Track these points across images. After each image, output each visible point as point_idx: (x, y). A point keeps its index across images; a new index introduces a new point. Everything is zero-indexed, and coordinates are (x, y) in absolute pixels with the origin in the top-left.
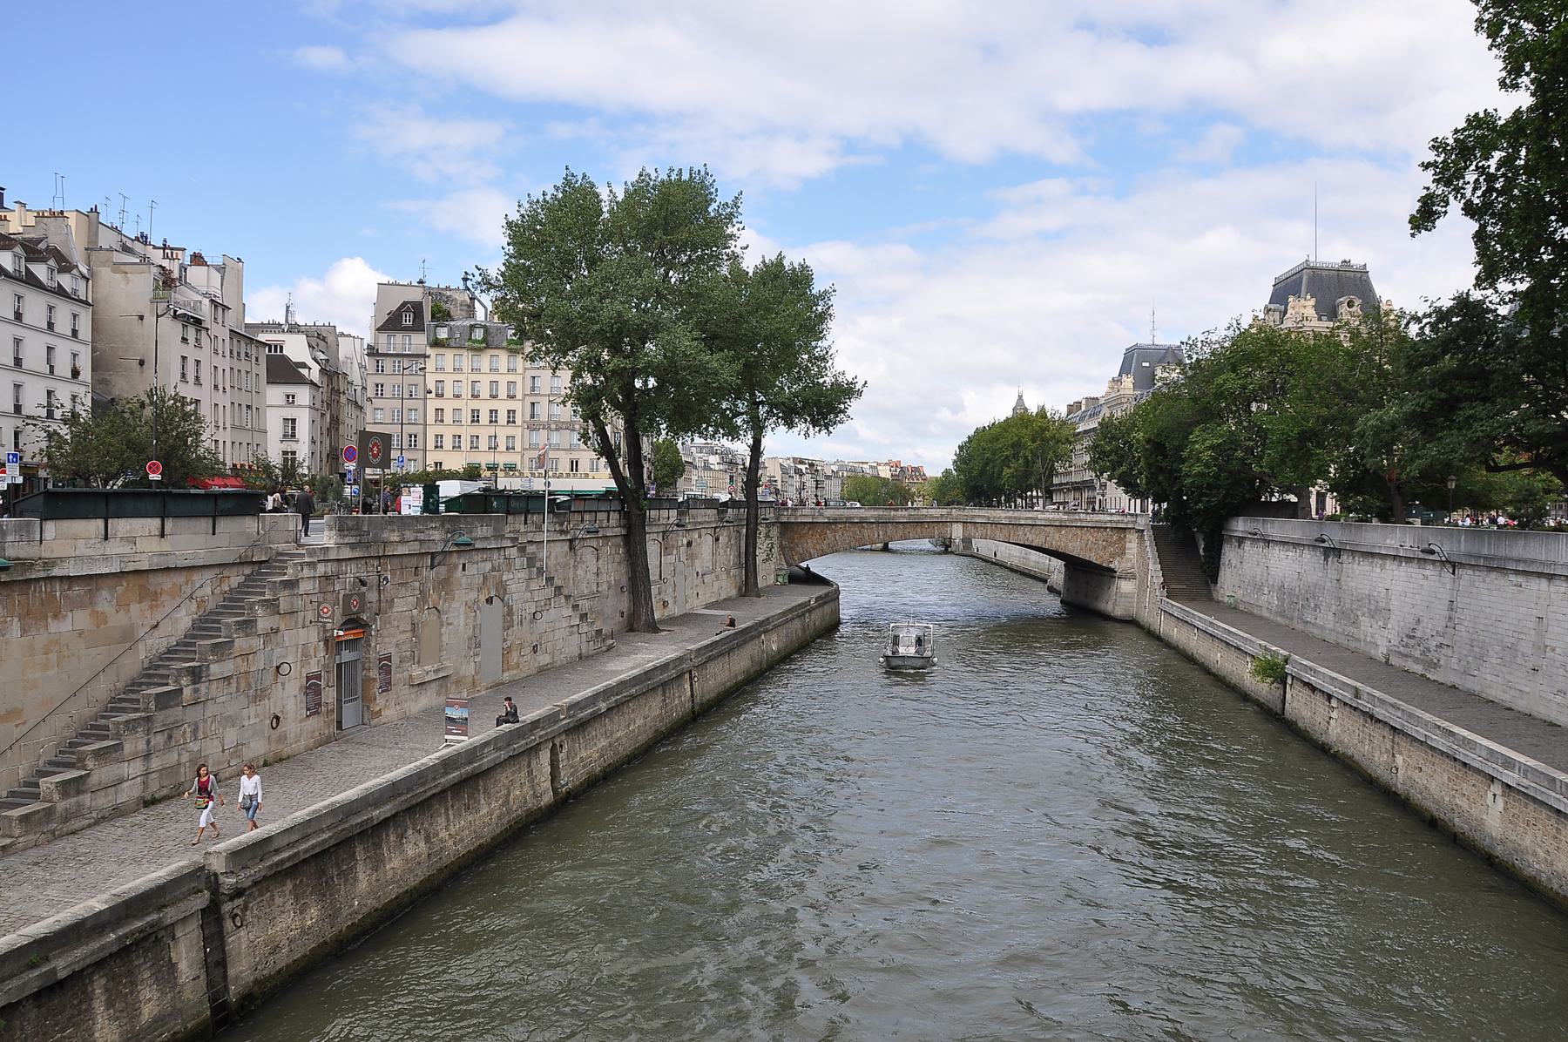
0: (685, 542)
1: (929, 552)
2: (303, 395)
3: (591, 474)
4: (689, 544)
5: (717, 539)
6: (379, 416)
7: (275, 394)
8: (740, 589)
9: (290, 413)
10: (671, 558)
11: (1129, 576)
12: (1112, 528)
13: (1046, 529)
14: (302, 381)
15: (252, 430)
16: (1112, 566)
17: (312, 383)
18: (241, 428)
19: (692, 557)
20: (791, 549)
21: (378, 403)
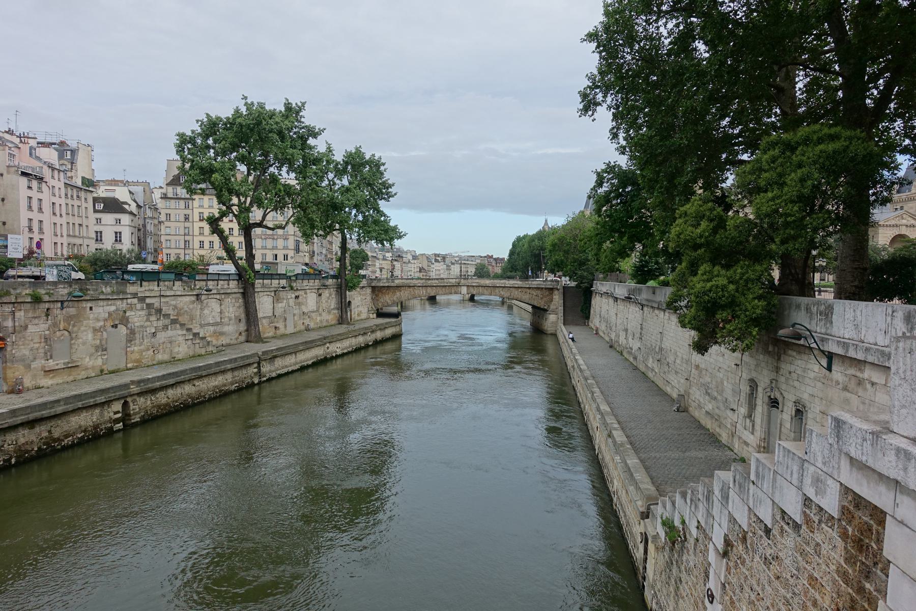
0: (293, 296)
2: (125, 219)
4: (297, 297)
5: (320, 295)
6: (168, 231)
7: (109, 218)
9: (118, 229)
10: (280, 305)
12: (546, 289)
14: (124, 211)
15: (83, 237)
17: (131, 213)
18: (75, 236)
19: (299, 304)
20: (378, 300)
21: (167, 224)
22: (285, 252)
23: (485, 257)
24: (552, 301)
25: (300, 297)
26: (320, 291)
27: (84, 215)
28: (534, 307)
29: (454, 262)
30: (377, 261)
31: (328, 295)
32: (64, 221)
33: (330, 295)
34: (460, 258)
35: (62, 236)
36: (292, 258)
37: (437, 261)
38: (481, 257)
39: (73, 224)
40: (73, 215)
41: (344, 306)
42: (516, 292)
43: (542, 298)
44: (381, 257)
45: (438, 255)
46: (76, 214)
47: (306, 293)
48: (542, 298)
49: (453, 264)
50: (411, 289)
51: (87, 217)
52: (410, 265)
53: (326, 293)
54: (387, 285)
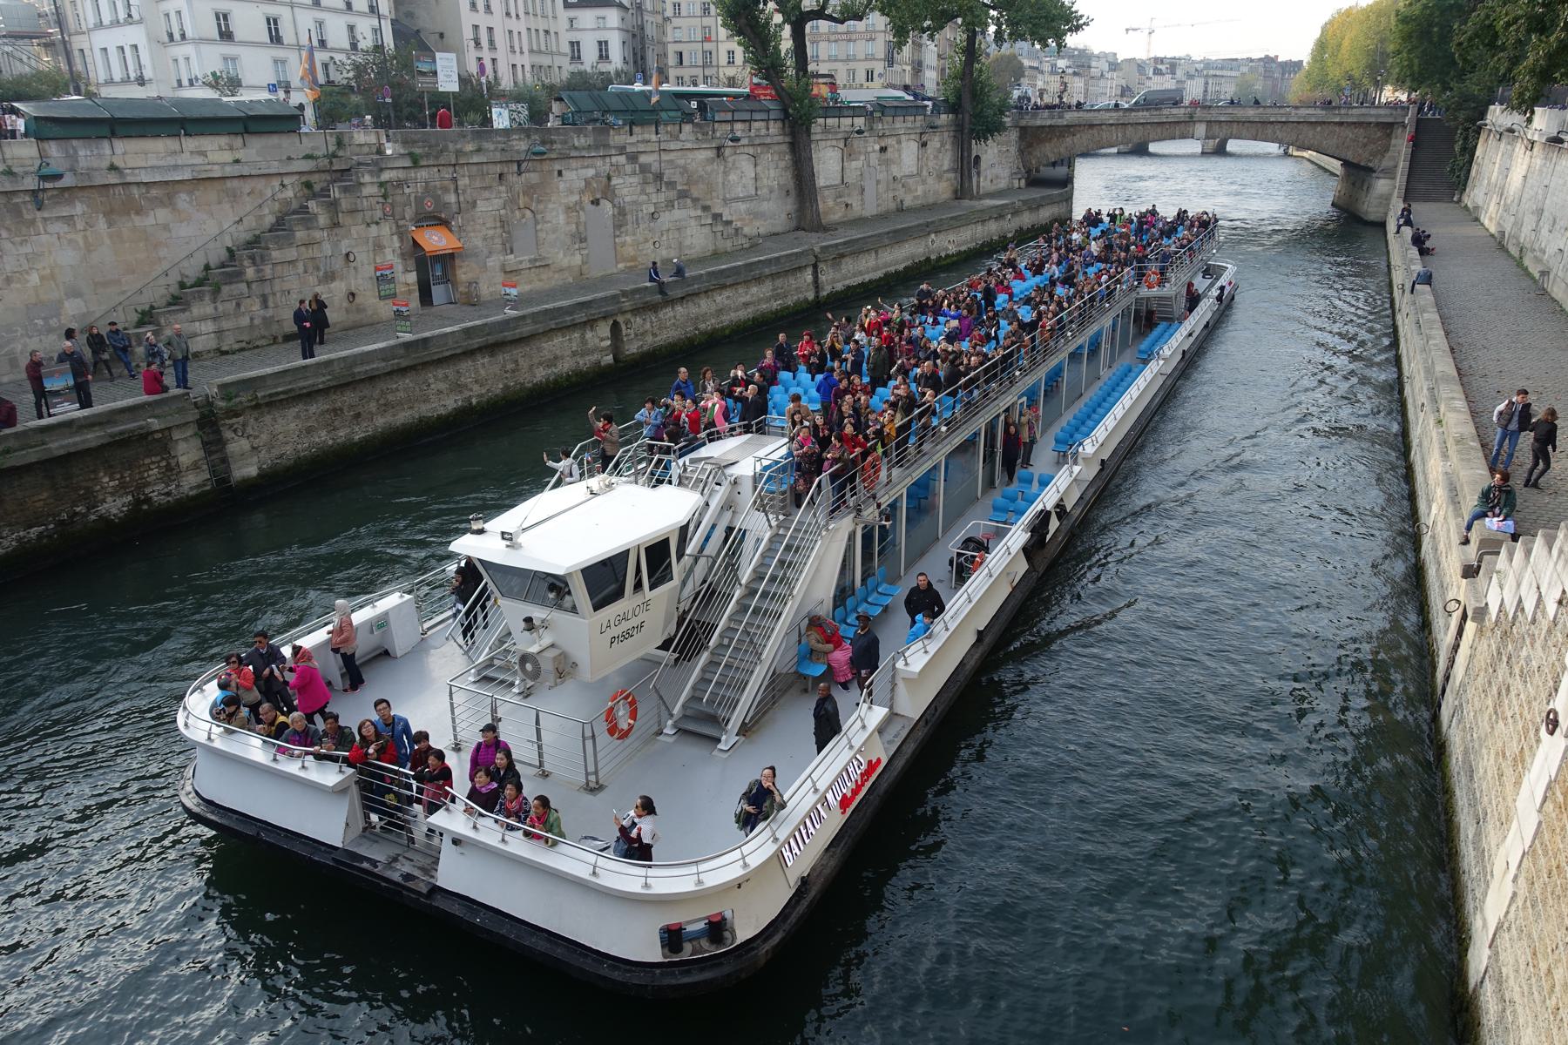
0: (877, 147)
1: (1192, 156)
3: (866, 84)
4: (883, 150)
5: (924, 145)
6: (678, 35)
8: (955, 192)
9: (602, 36)
10: (854, 164)
11: (1390, 173)
12: (1378, 124)
13: (1301, 126)
15: (552, 53)
16: (1370, 165)
18: (540, 52)
19: (887, 163)
21: (676, 22)
22: (869, 65)
23: (1260, 59)
24: (1387, 150)
25: (889, 150)
26: (925, 138)
27: (550, 14)
28: (1346, 164)
29: (1192, 72)
30: (1040, 76)
31: (938, 145)
32: (519, 26)
33: (943, 145)
34: (1208, 64)
35: (522, 53)
36: (880, 75)
37: (1157, 72)
38: (1252, 60)
39: (537, 30)
40: (535, 15)
41: (966, 166)
42: (1311, 134)
43: (1365, 145)
44: (1047, 68)
45: (1161, 60)
46: (539, 12)
47: (899, 142)
48: (1365, 145)
49: (1190, 77)
50: (1095, 131)
51: (555, 18)
52: (1102, 83)
53: (935, 142)
54: (1048, 123)
